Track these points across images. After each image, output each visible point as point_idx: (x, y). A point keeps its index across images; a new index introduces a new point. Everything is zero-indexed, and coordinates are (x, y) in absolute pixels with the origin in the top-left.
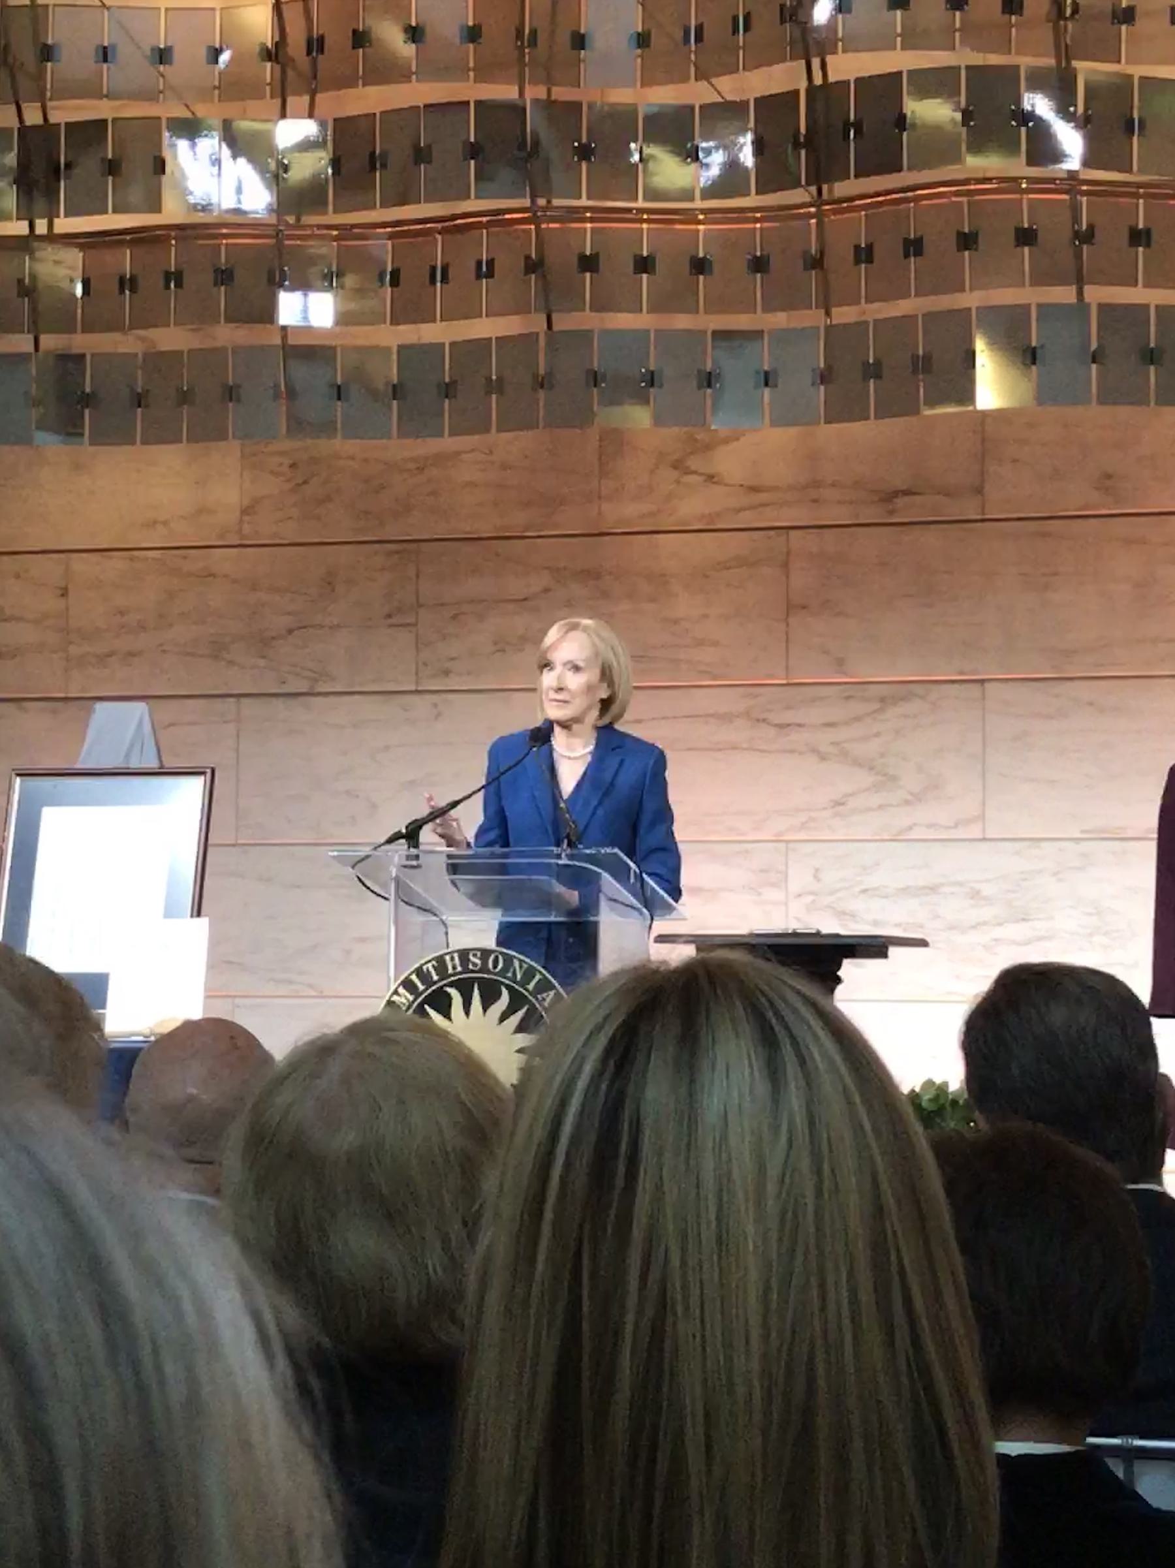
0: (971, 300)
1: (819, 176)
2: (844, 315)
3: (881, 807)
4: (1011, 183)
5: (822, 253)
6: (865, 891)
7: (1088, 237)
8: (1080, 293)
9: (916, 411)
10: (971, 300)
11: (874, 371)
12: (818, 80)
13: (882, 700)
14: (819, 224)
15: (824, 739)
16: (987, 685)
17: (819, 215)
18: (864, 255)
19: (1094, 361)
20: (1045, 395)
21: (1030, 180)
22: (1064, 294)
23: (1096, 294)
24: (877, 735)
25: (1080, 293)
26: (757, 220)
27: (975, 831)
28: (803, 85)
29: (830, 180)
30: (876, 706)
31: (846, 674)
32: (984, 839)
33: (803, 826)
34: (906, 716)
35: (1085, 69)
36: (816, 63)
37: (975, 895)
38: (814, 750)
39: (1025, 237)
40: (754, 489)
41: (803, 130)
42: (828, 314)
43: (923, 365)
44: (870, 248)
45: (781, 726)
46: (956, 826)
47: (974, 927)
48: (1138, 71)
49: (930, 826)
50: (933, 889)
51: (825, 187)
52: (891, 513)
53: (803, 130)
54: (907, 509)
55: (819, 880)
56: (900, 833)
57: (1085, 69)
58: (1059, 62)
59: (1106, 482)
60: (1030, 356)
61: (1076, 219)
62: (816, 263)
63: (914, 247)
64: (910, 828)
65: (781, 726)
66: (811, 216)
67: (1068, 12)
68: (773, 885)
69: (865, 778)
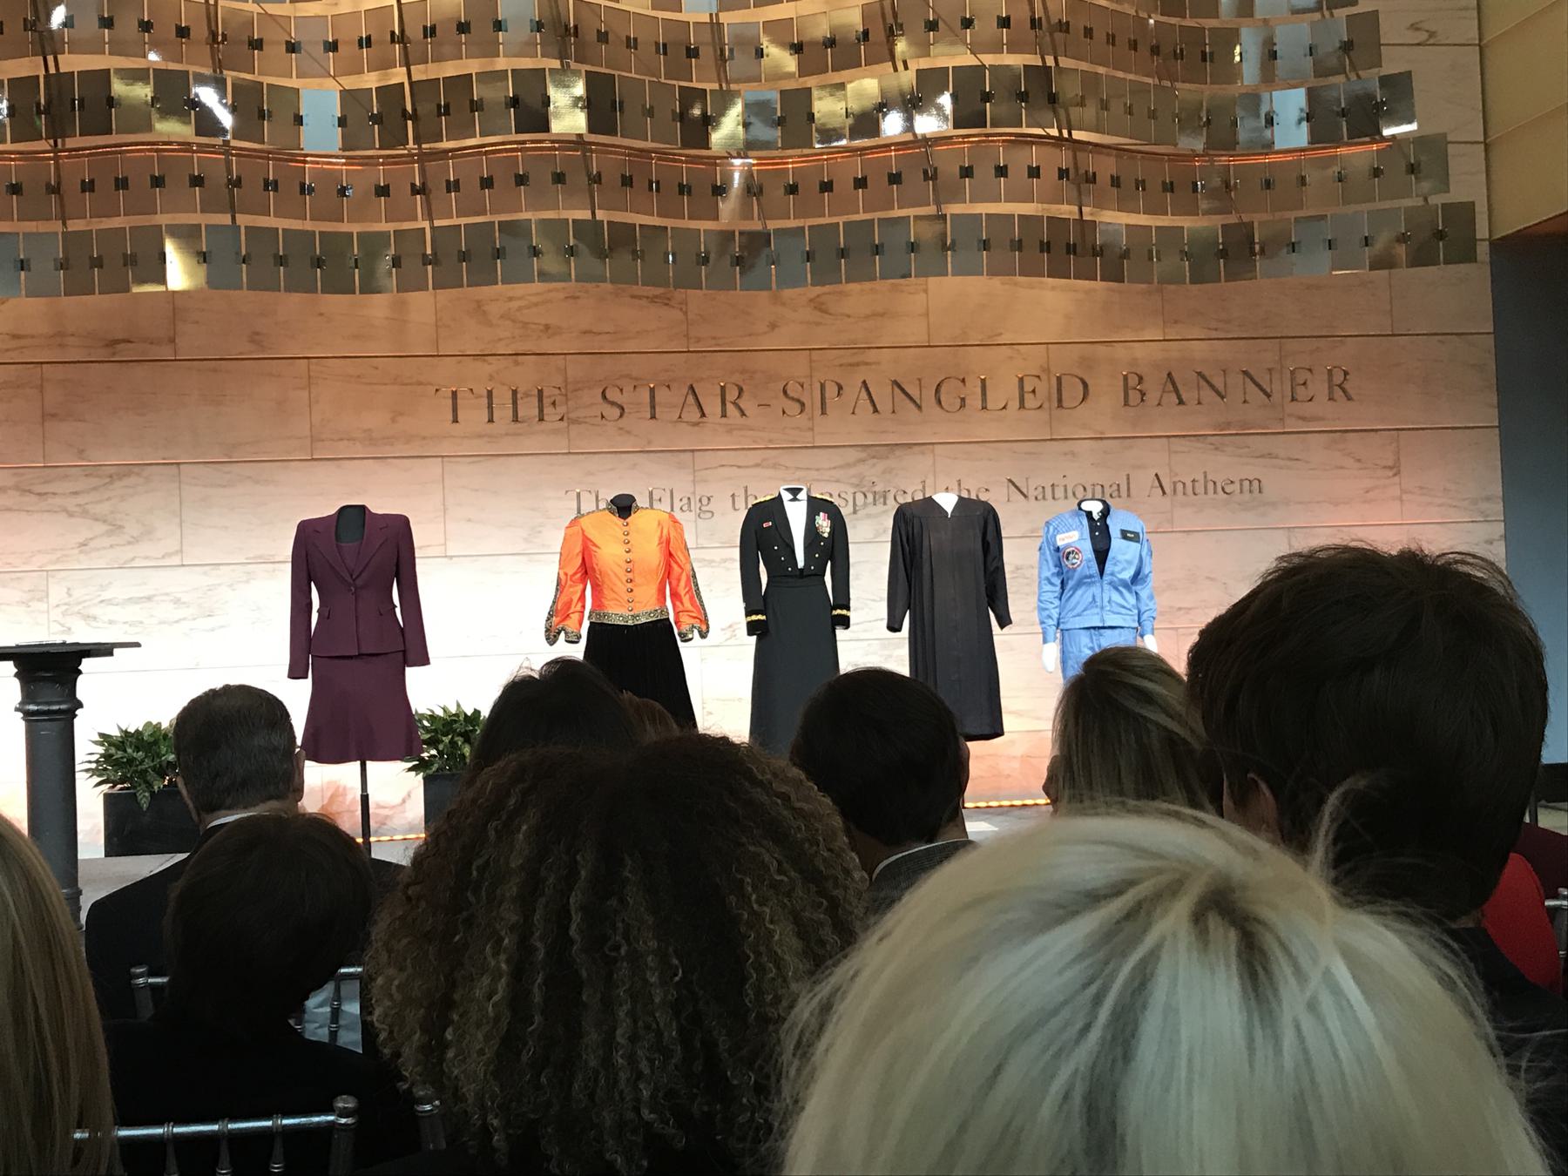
0: (163, 219)
1: (57, 131)
2: (75, 225)
3: (111, 546)
4: (187, 147)
5: (59, 184)
6: (102, 601)
7: (238, 183)
8: (234, 218)
9: (127, 290)
10: (163, 219)
11: (98, 263)
12: (52, 70)
13: (111, 476)
14: (57, 164)
15: (71, 502)
16: (181, 466)
17: (56, 159)
18: (88, 187)
19: (244, 262)
20: (212, 282)
21: (198, 145)
22: (225, 219)
23: (243, 220)
24: (109, 499)
25: (234, 218)
26: (12, 160)
27: (176, 560)
28: (42, 73)
29: (64, 137)
30: (108, 480)
31: (83, 460)
32: (183, 565)
33: (58, 561)
34: (127, 487)
35: (229, 75)
36: (50, 59)
37: (177, 601)
38: (65, 510)
39: (197, 181)
40: (15, 337)
41: (43, 101)
42: (64, 224)
43: (130, 261)
44: (92, 182)
45: (39, 494)
46: (163, 557)
47: (177, 622)
48: (267, 80)
49: (146, 558)
50: (149, 598)
51: (59, 141)
52: (114, 354)
53: (43, 101)
54: (125, 352)
55: (70, 595)
56: (125, 563)
57: (229, 75)
58: (215, 71)
59: (255, 338)
60: (203, 257)
61: (229, 171)
62: (55, 190)
63: (122, 184)
64: (133, 559)
65: (39, 494)
66: (50, 159)
67: (220, 39)
68: (40, 600)
69: (100, 528)
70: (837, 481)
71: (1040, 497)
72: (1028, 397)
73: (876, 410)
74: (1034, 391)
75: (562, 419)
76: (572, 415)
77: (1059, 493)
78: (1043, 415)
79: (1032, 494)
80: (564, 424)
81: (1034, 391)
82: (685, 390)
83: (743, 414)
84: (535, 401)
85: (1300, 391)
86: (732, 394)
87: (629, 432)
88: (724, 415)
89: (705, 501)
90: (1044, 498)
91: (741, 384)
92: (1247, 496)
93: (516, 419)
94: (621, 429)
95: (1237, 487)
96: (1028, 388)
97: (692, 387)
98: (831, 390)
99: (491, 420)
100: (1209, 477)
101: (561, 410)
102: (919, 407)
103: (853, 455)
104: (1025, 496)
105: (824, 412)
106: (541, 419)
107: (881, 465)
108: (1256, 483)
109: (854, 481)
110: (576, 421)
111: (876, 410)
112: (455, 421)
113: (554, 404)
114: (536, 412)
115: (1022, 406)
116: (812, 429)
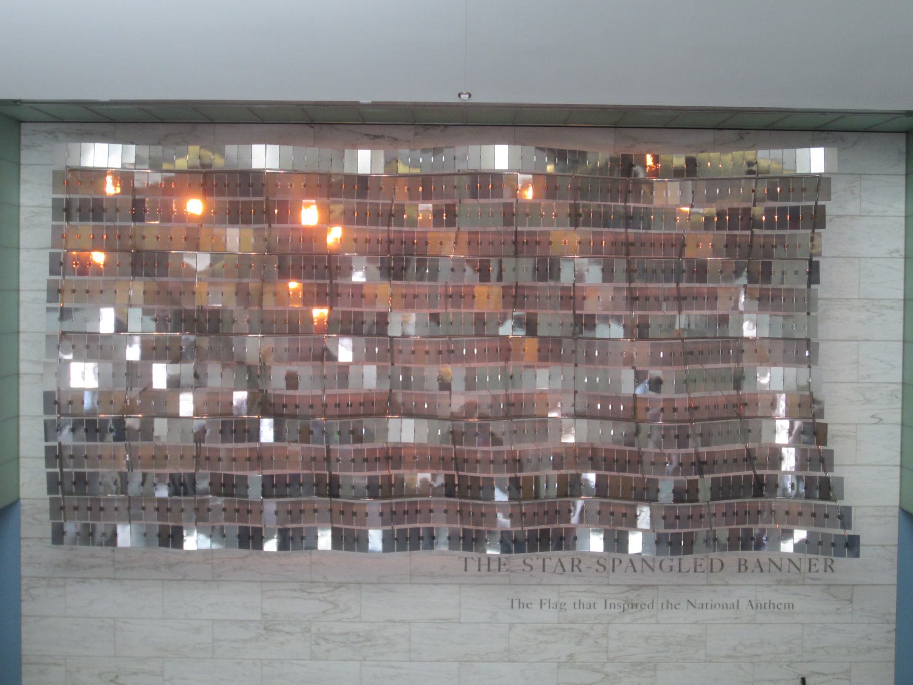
70: (618, 599)
71: (701, 608)
72: (699, 569)
73: (635, 571)
74: (701, 565)
75: (507, 571)
76: (513, 569)
77: (709, 606)
78: (703, 575)
79: (697, 606)
80: (508, 573)
81: (701, 565)
82: (557, 560)
83: (580, 571)
84: (497, 563)
85: (813, 568)
86: (576, 562)
87: (533, 576)
88: (572, 571)
89: (563, 605)
90: (702, 608)
91: (580, 558)
92: (787, 610)
93: (489, 570)
94: (531, 575)
95: (783, 606)
96: (698, 563)
97: (560, 559)
98: (617, 562)
99: (479, 570)
100: (772, 602)
101: (507, 567)
102: (653, 570)
103: (624, 589)
104: (694, 607)
105: (613, 571)
106: (499, 570)
107: (637, 593)
108: (791, 605)
109: (625, 599)
110: (512, 572)
111: (635, 571)
112: (466, 570)
113: (504, 564)
114: (497, 567)
115: (695, 571)
116: (608, 578)
